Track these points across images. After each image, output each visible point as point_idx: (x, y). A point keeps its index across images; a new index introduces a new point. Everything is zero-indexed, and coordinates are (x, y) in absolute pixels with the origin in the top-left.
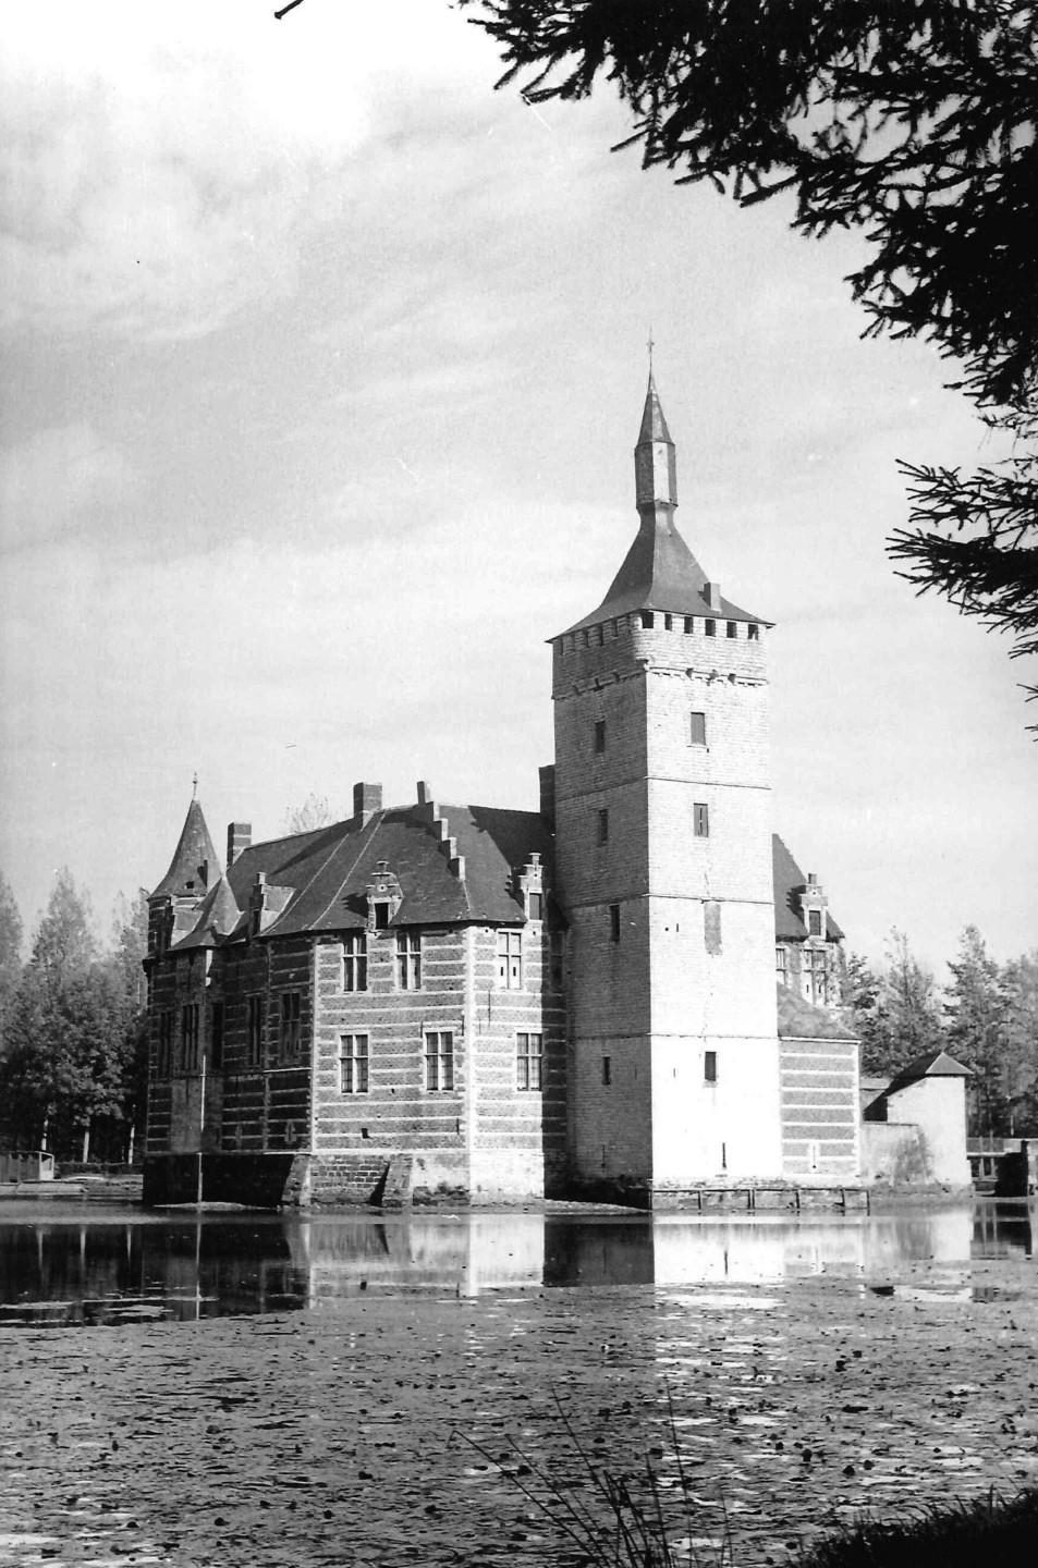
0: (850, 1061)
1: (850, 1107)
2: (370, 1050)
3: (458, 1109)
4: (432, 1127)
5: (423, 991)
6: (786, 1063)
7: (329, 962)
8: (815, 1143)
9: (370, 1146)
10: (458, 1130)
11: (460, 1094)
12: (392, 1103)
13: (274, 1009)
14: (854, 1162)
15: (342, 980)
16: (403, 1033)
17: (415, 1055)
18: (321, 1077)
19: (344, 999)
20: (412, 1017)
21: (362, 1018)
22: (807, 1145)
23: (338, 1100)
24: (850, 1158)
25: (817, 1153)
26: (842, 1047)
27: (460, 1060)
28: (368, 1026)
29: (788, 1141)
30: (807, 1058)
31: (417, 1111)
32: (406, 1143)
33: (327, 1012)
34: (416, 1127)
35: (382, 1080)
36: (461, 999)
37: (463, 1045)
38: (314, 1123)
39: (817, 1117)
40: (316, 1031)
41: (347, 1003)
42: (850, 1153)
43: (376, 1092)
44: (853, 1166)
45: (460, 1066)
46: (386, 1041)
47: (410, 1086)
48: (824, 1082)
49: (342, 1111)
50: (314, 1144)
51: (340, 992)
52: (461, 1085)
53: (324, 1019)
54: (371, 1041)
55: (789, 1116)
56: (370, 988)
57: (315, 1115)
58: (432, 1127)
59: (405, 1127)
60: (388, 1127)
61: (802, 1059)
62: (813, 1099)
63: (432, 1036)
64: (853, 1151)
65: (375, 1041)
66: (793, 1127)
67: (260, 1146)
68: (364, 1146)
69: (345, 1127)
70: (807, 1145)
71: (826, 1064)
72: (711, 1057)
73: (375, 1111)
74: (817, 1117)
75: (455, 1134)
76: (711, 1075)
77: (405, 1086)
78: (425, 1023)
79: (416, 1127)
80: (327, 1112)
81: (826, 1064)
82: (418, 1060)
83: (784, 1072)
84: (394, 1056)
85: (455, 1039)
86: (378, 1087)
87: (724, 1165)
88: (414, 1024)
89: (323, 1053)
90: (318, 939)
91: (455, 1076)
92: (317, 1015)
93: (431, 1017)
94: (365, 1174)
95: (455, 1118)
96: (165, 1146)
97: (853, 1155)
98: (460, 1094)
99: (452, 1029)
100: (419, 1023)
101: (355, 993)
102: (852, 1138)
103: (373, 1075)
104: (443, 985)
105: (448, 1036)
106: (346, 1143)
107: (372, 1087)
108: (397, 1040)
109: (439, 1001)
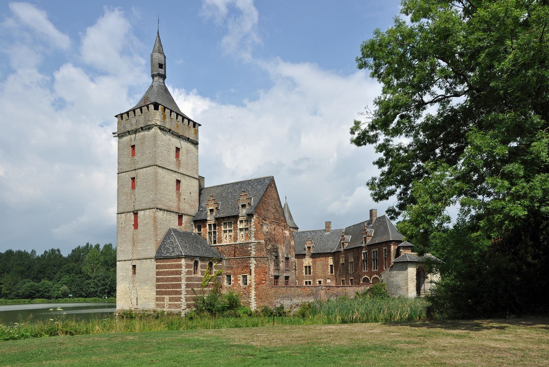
0: (181, 265)
1: (180, 283)
6: (158, 267)
8: (167, 297)
14: (181, 304)
22: (164, 298)
24: (180, 303)
25: (168, 301)
26: (178, 260)
29: (158, 296)
30: (165, 265)
39: (168, 286)
42: (180, 301)
44: (181, 305)
48: (172, 273)
55: (158, 287)
61: (163, 265)
62: (167, 280)
64: (181, 300)
66: (159, 291)
70: (164, 298)
71: (171, 266)
72: (134, 267)
74: (168, 286)
76: (134, 273)
81: (171, 266)
83: (157, 270)
87: (137, 304)
97: (181, 301)
102: (181, 295)
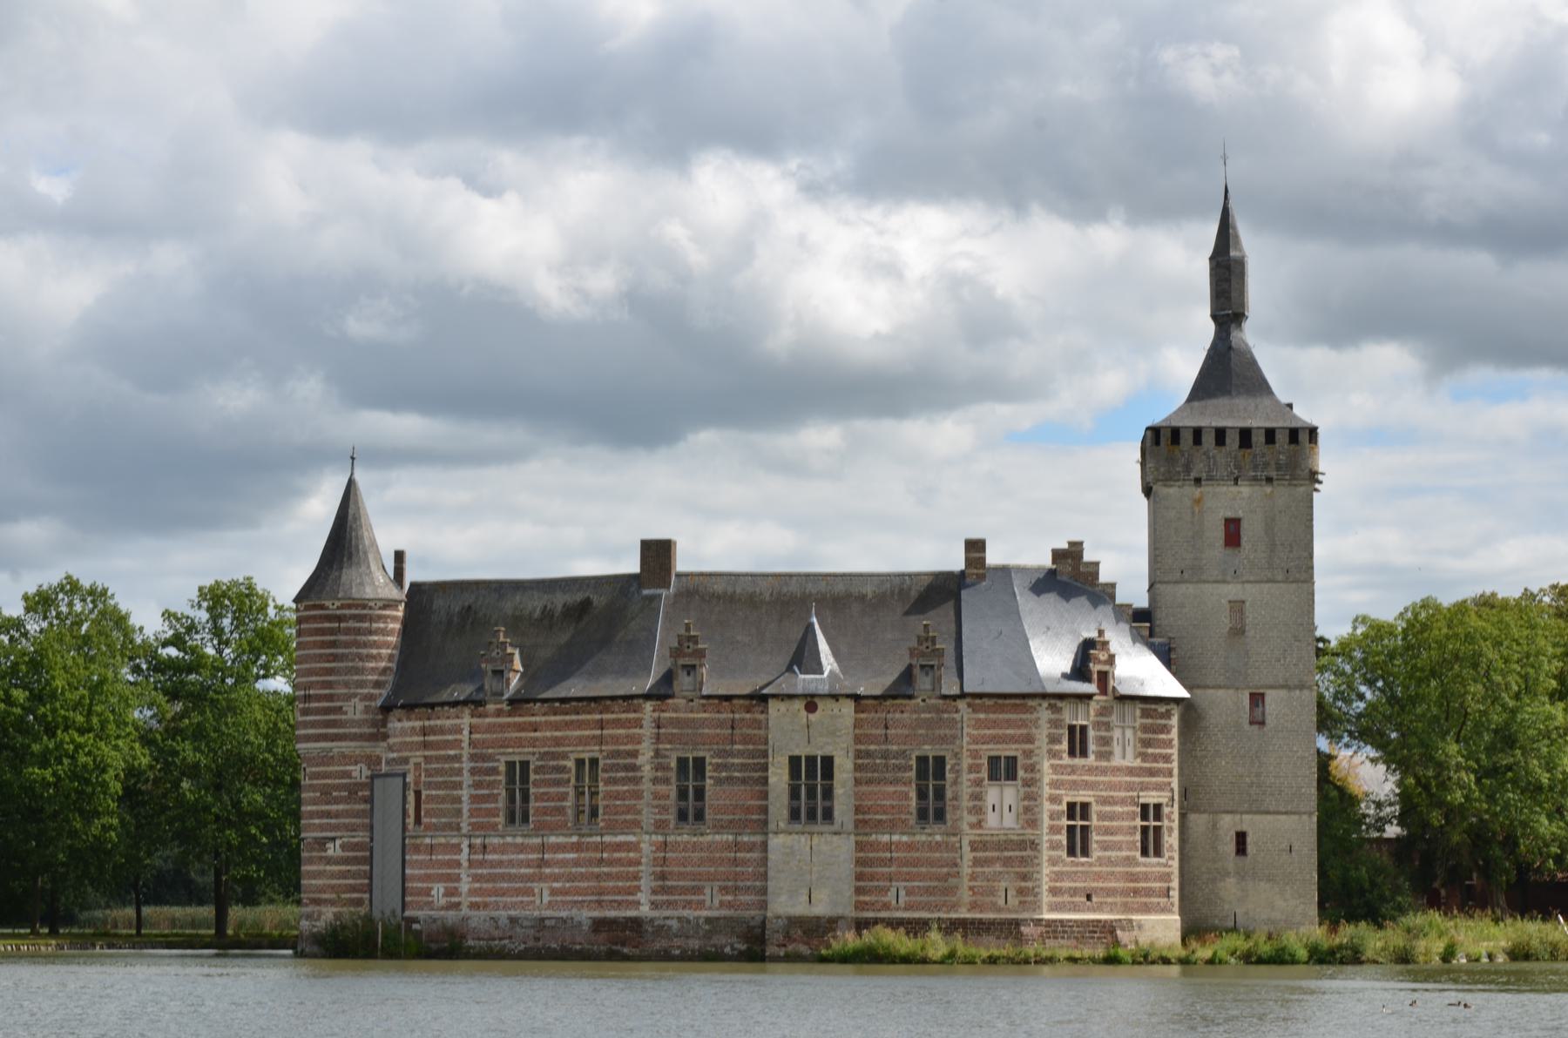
2: (1094, 817)
3: (1166, 877)
4: (1149, 892)
5: (1138, 763)
7: (1056, 727)
9: (1094, 910)
10: (1168, 897)
11: (1170, 863)
12: (1114, 869)
13: (971, 769)
15: (1065, 746)
16: (1123, 802)
17: (1132, 824)
18: (1051, 841)
19: (1070, 766)
20: (1130, 786)
21: (1088, 786)
23: (1065, 865)
27: (1170, 829)
28: (1091, 793)
31: (1133, 877)
32: (1127, 908)
33: (1055, 777)
34: (1136, 892)
35: (1105, 847)
36: (1170, 774)
37: (1173, 817)
38: (1045, 887)
40: (1046, 796)
41: (1073, 770)
43: (1099, 858)
45: (1170, 836)
46: (1108, 808)
47: (1128, 853)
49: (1071, 876)
50: (1045, 907)
51: (1066, 760)
52: (1170, 854)
53: (1055, 784)
54: (1095, 808)
56: (1092, 757)
57: (1045, 879)
58: (1149, 892)
59: (1125, 893)
60: (1111, 892)
63: (1145, 807)
65: (1100, 808)
67: (954, 907)
68: (1090, 910)
69: (1074, 892)
73: (1099, 876)
75: (1166, 900)
77: (1124, 854)
78: (1141, 794)
79: (1136, 892)
80: (1058, 876)
82: (1135, 827)
84: (1115, 823)
85: (1166, 810)
86: (1100, 854)
88: (1131, 794)
89: (1051, 817)
90: (1045, 704)
91: (1166, 845)
92: (1046, 780)
93: (1144, 787)
94: (1093, 938)
95: (1165, 885)
96: (763, 905)
98: (1170, 863)
99: (1164, 801)
100: (1135, 794)
101: (1078, 761)
103: (1097, 842)
104: (1155, 758)
105: (1158, 807)
106: (1075, 908)
107: (1096, 853)
108: (1118, 809)
109: (1152, 773)
